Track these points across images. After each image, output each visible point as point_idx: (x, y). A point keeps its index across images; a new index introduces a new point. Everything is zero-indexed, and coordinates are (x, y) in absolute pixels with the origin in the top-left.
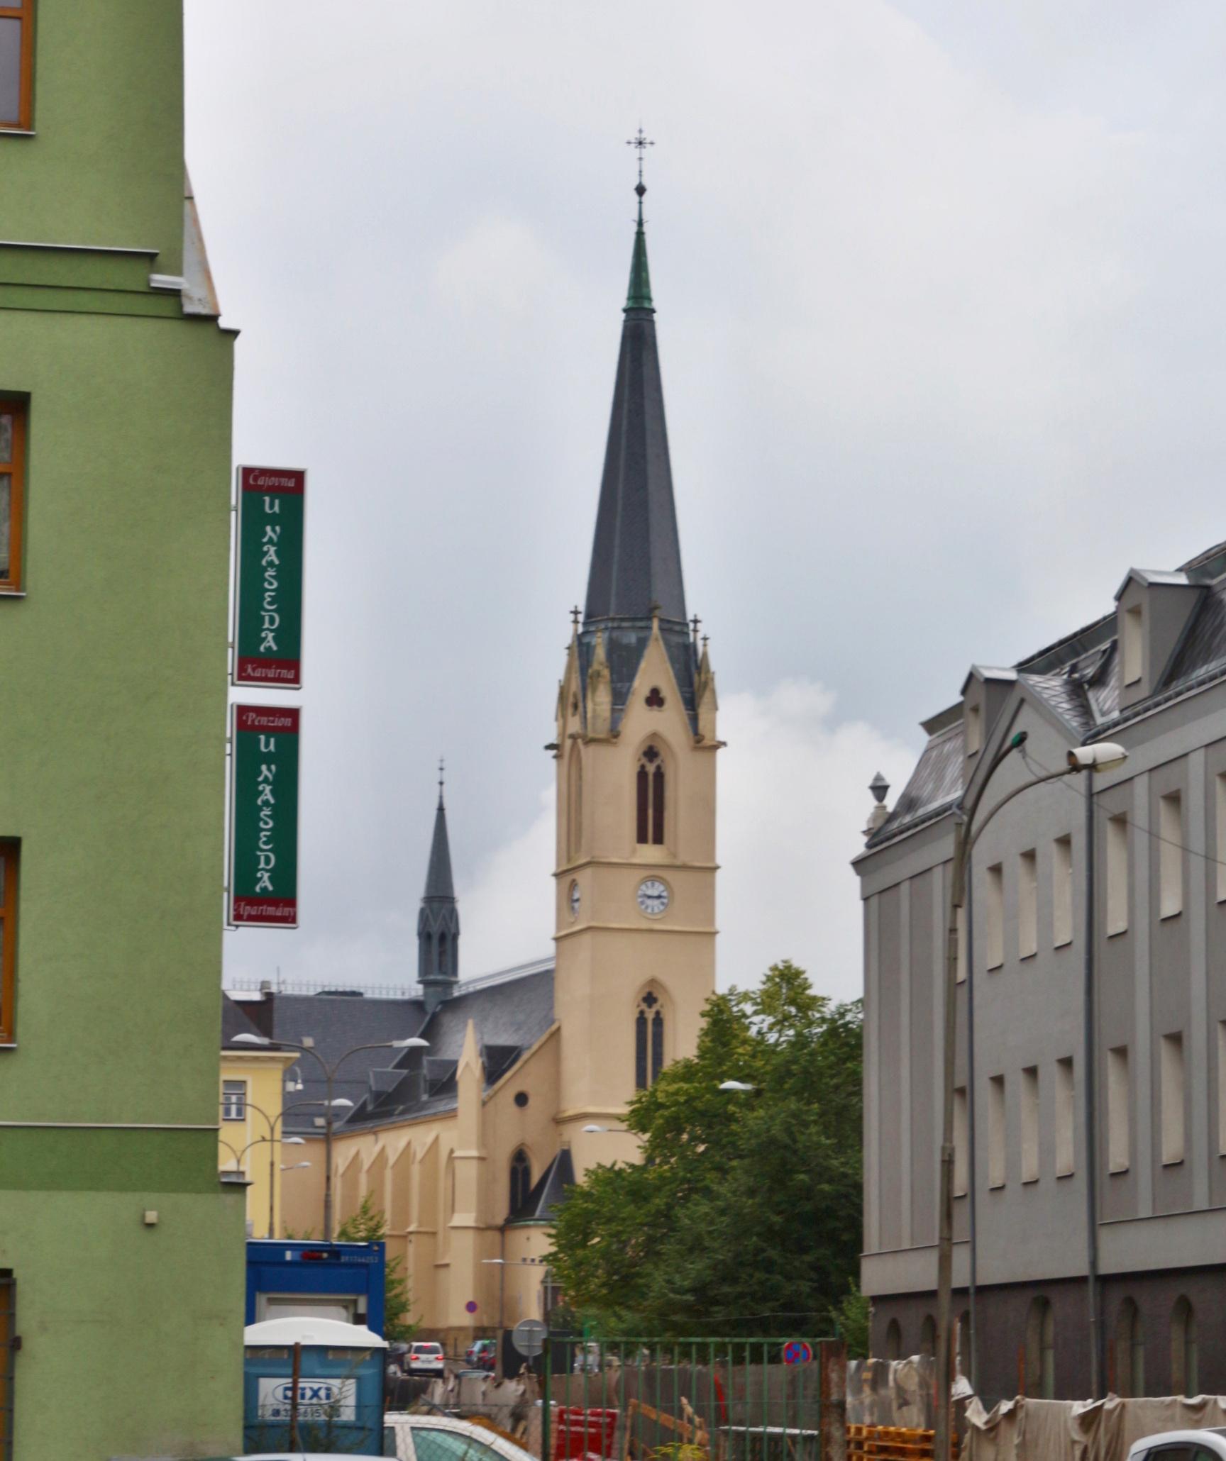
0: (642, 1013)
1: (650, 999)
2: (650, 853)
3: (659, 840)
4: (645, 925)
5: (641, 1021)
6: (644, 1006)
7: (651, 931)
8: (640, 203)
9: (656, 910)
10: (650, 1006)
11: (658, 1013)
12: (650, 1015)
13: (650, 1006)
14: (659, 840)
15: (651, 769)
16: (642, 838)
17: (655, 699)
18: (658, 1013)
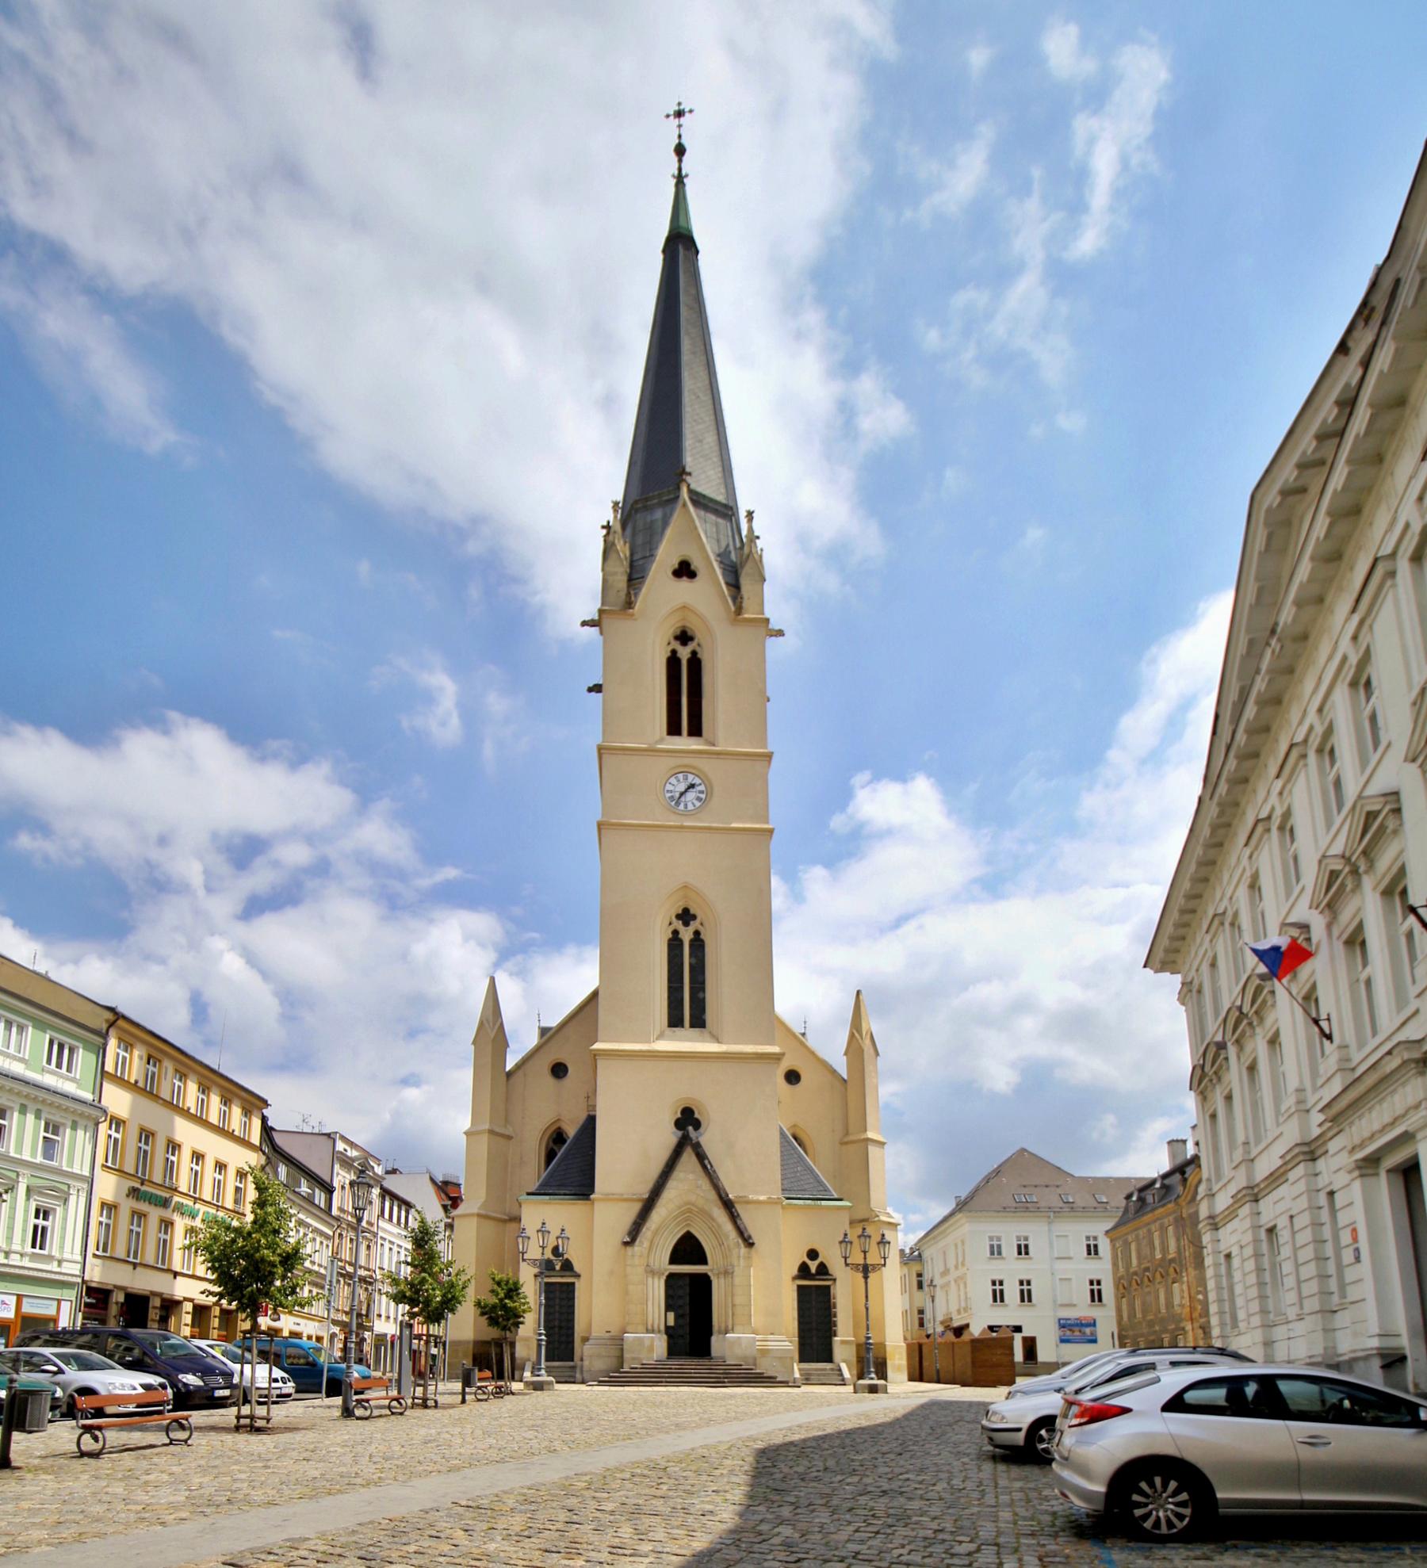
0: (676, 932)
1: (686, 916)
2: (684, 742)
3: (696, 730)
4: (673, 821)
5: (675, 943)
6: (679, 925)
7: (682, 827)
8: (680, 136)
9: (690, 807)
10: (686, 924)
11: (697, 933)
12: (686, 935)
13: (686, 924)
14: (696, 730)
15: (684, 653)
16: (674, 729)
17: (684, 570)
18: (697, 933)
